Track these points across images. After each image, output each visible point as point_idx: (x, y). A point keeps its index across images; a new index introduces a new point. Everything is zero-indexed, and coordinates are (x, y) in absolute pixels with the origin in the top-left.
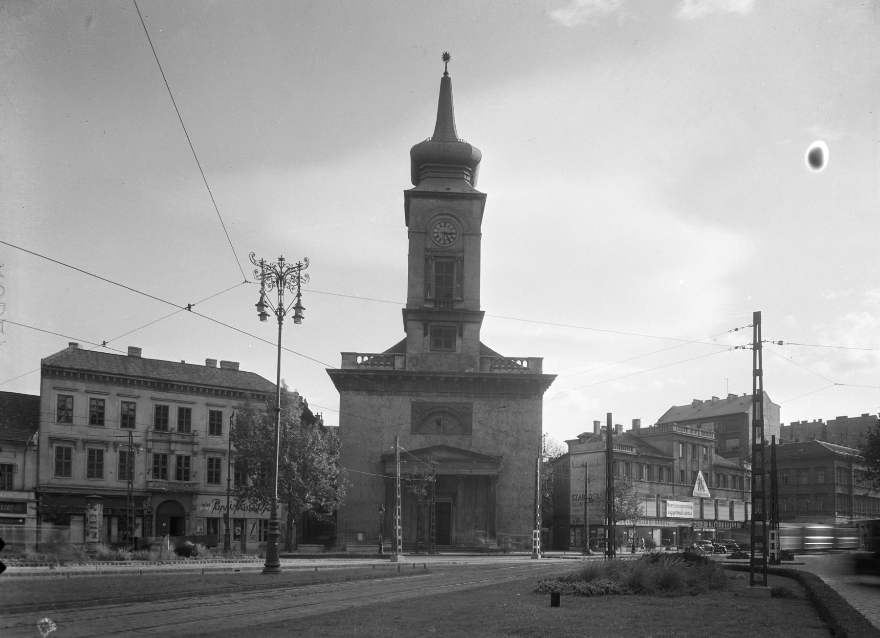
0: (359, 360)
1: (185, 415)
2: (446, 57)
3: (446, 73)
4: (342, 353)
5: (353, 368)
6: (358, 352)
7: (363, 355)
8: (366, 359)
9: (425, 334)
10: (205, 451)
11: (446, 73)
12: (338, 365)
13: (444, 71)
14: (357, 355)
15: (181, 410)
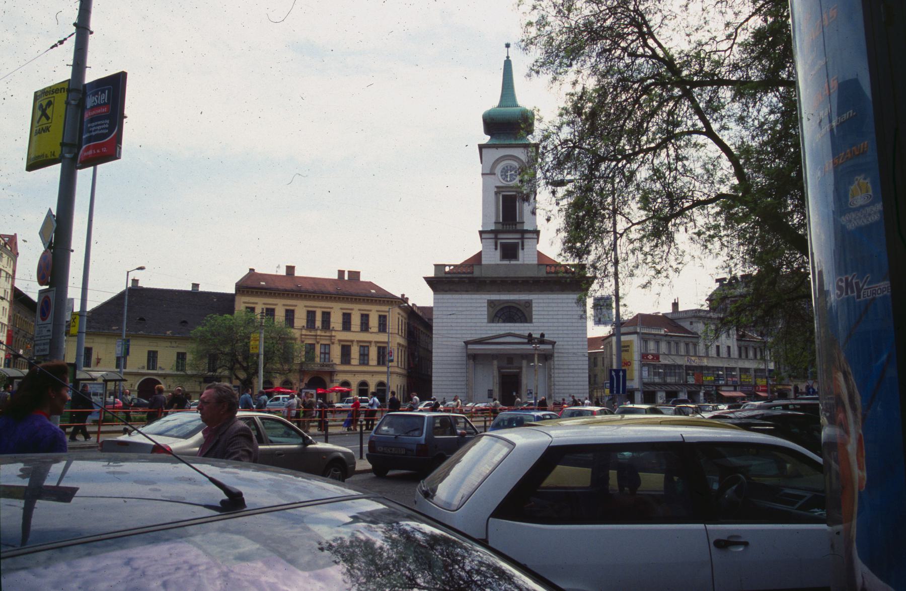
0: (447, 269)
1: (326, 316)
2: (508, 46)
3: (508, 57)
4: (436, 265)
5: (443, 275)
6: (446, 264)
7: (450, 266)
8: (452, 267)
9: (496, 249)
10: (340, 341)
11: (508, 57)
12: (432, 274)
13: (506, 55)
14: (445, 266)
15: (324, 313)
